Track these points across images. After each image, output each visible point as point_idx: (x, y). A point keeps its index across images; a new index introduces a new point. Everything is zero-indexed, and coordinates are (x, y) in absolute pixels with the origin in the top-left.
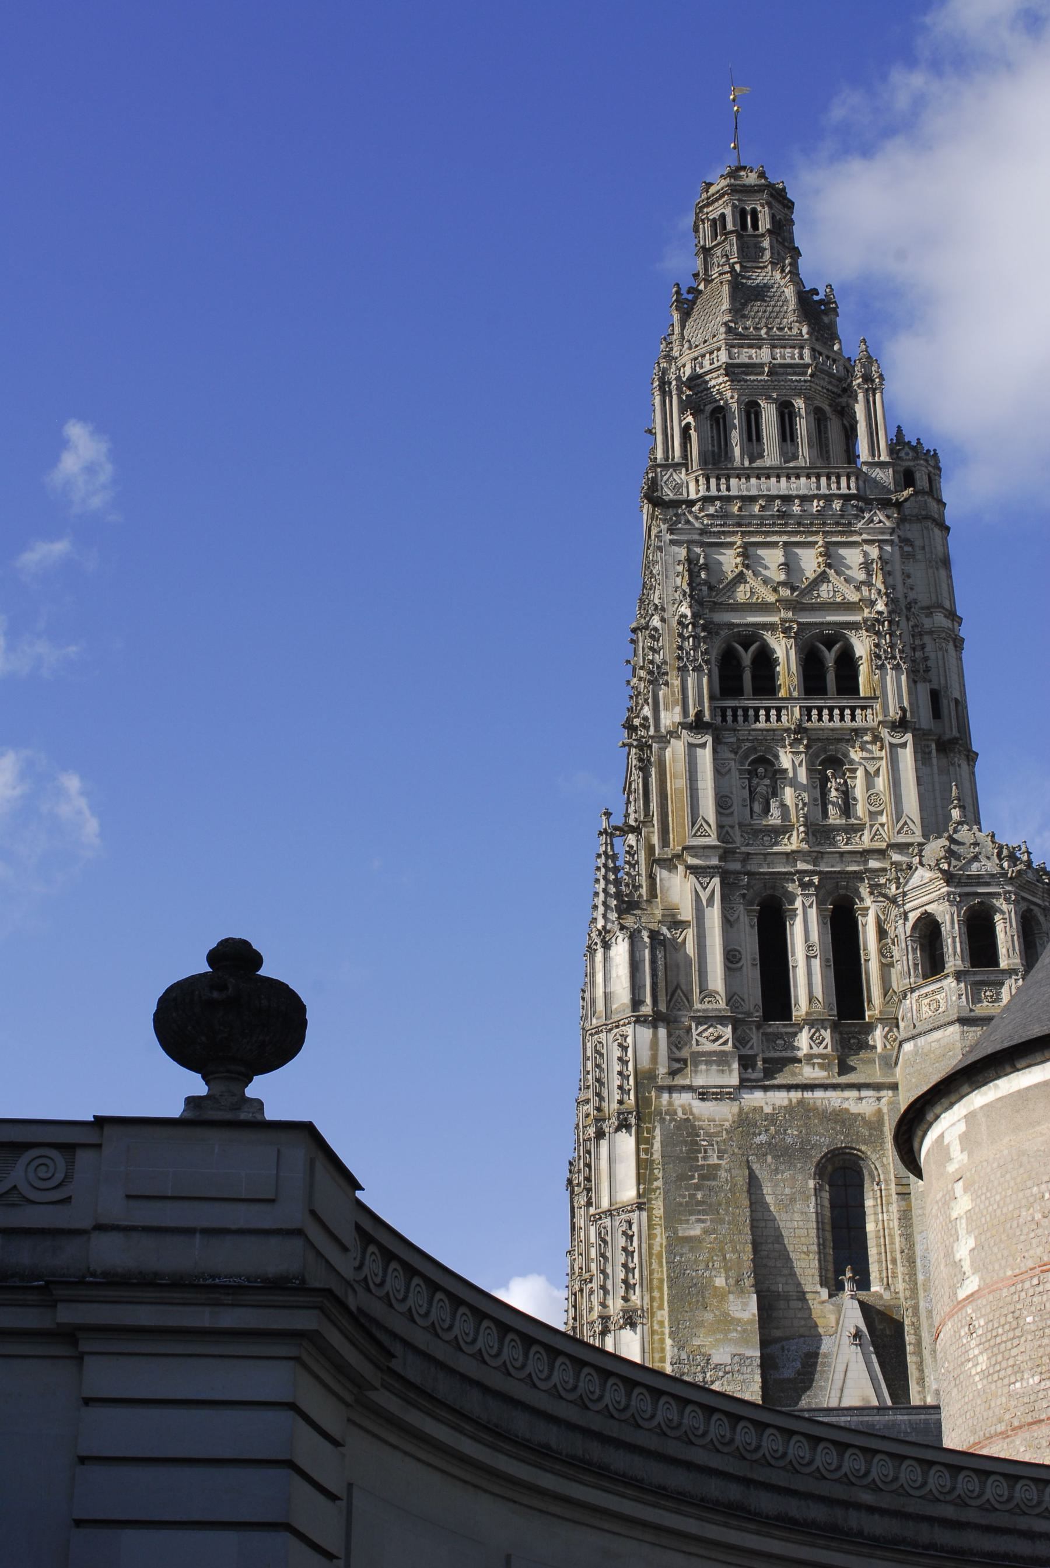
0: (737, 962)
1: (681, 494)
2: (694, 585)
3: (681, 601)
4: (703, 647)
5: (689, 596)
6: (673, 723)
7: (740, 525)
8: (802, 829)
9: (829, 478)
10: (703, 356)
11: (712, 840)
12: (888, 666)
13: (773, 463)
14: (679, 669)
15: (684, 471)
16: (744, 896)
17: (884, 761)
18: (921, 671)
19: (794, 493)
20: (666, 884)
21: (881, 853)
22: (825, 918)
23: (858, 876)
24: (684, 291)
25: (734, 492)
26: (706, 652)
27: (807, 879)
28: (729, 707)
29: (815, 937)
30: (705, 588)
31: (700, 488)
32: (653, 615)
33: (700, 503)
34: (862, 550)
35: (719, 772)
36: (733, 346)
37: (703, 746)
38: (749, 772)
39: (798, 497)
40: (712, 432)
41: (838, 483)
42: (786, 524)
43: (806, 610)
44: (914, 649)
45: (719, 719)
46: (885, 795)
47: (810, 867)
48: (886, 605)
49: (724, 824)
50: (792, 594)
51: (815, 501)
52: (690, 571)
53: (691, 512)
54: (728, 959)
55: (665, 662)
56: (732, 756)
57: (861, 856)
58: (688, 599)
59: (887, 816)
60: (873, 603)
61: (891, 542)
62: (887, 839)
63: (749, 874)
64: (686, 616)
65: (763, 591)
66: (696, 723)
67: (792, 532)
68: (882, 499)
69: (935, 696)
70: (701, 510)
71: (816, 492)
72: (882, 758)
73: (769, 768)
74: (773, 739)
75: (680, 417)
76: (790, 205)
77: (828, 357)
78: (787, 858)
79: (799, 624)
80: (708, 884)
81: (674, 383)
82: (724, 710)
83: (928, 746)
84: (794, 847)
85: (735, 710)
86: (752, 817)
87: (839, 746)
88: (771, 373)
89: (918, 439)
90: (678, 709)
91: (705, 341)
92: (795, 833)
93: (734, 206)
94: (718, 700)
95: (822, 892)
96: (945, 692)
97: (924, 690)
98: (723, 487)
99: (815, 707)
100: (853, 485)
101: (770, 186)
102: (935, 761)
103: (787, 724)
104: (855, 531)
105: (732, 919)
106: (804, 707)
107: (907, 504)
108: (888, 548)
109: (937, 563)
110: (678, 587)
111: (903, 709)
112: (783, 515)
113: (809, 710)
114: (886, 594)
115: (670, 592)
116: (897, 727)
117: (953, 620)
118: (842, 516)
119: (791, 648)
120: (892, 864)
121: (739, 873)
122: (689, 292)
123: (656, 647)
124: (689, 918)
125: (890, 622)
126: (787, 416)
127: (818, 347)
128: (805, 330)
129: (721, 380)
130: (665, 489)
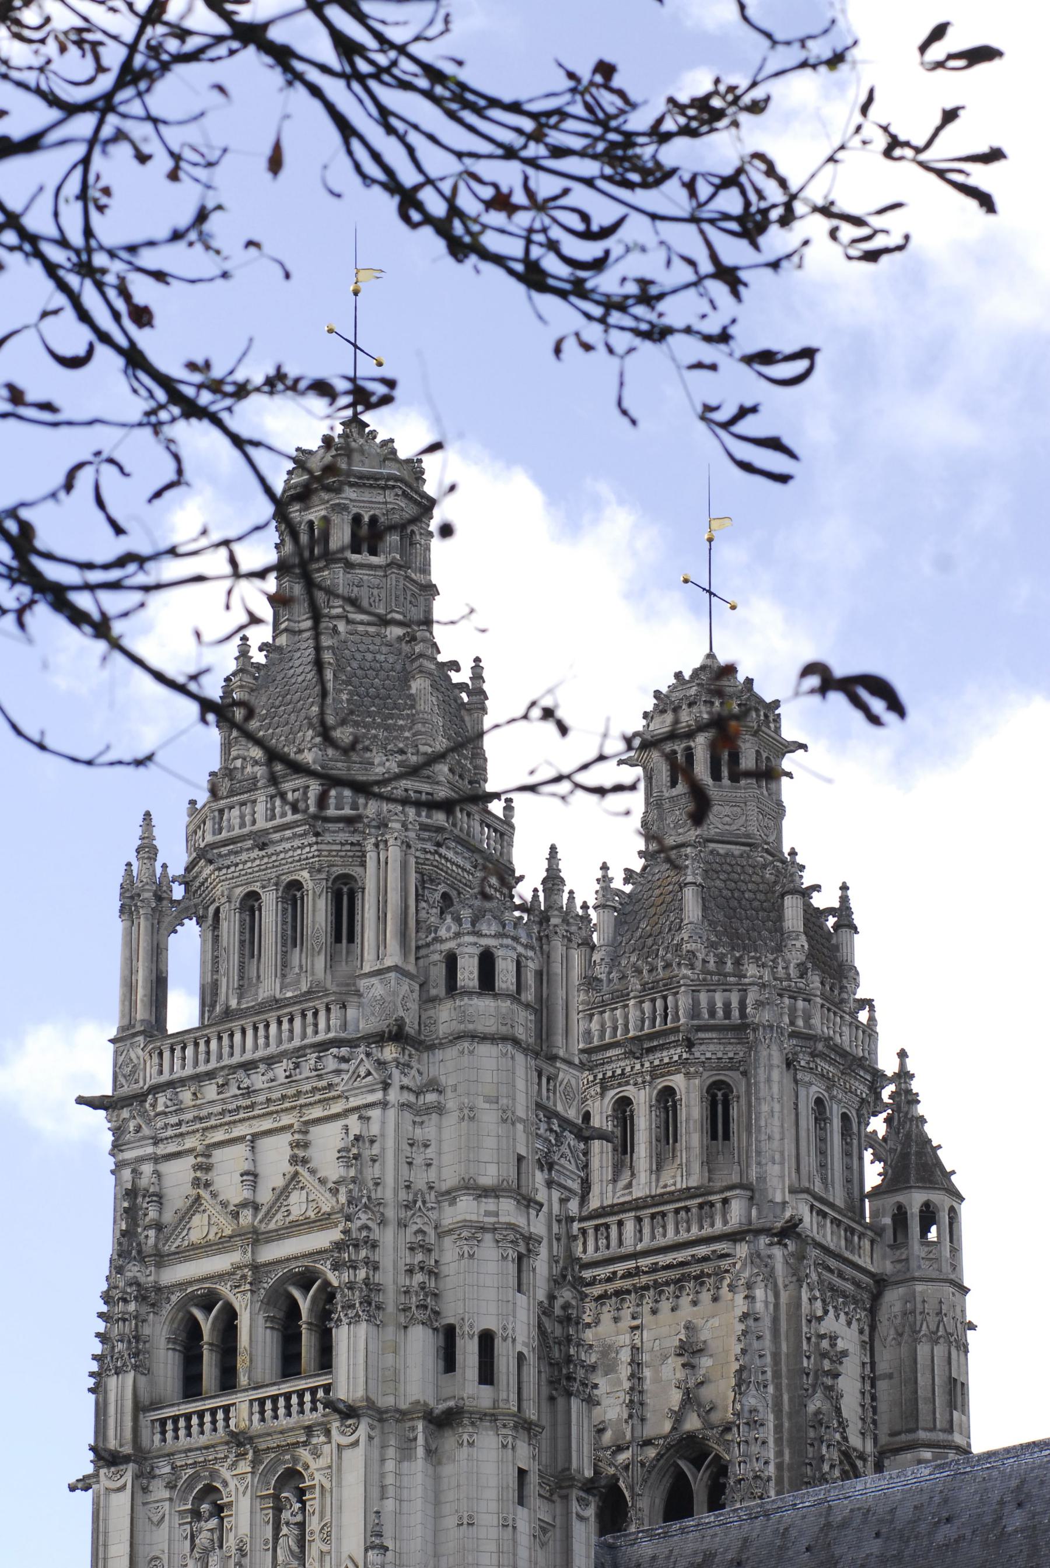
42: (252, 1106)
43: (273, 1241)
56: (166, 1494)
67: (264, 1115)
74: (216, 1458)
83: (413, 1429)
96: (461, 1327)
104: (339, 1097)
112: (249, 1092)
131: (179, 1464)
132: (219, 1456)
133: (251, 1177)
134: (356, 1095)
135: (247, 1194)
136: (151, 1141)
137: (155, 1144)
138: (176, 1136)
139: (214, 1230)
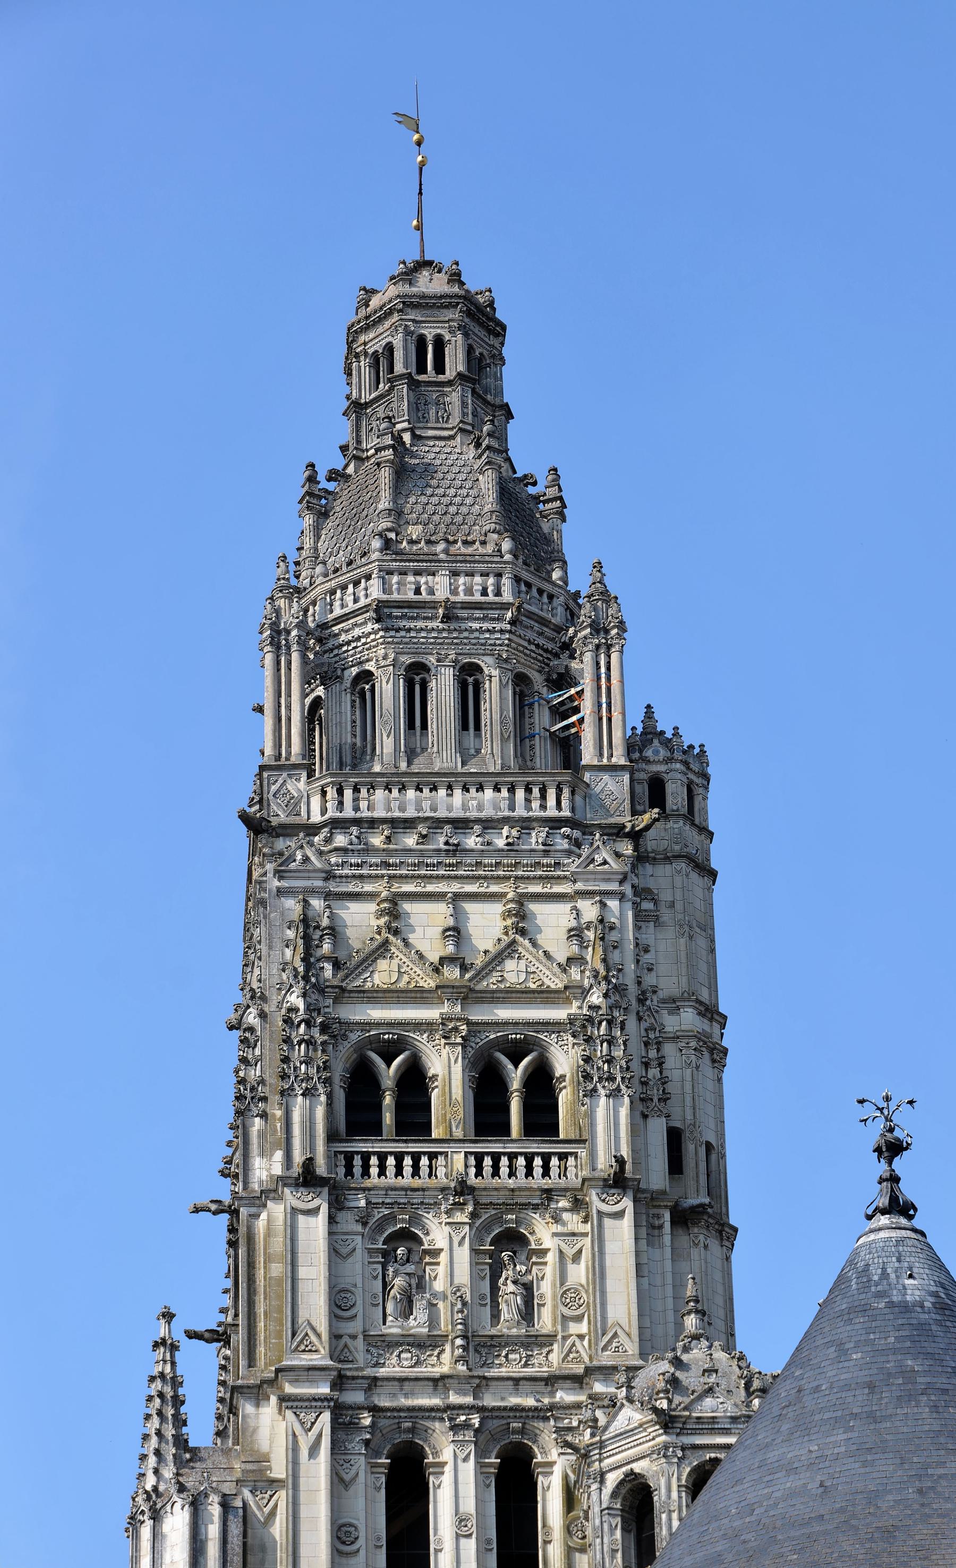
0: (352, 1543)
1: (298, 814)
2: (312, 960)
3: (291, 986)
4: (320, 1058)
5: (303, 978)
6: (271, 1176)
7: (387, 865)
8: (459, 1342)
9: (528, 790)
10: (344, 587)
11: (320, 1358)
12: (602, 1092)
13: (445, 765)
14: (282, 1093)
15: (304, 775)
16: (367, 1443)
17: (589, 1239)
18: (656, 1099)
19: (473, 814)
20: (252, 1422)
21: (578, 1381)
22: (487, 1478)
23: (540, 1414)
24: (321, 477)
25: (380, 813)
26: (326, 1067)
27: (463, 1418)
28: (357, 1153)
29: (469, 1505)
30: (328, 967)
31: (329, 805)
32: (248, 1007)
33: (326, 830)
34: (575, 908)
35: (336, 1253)
36: (390, 573)
37: (314, 1212)
38: (385, 1254)
39: (478, 821)
40: (353, 713)
41: (543, 797)
43: (483, 1002)
44: (646, 1065)
45: (342, 1171)
46: (587, 1292)
47: (468, 1400)
48: (606, 996)
49: (341, 1332)
50: (462, 976)
51: (506, 828)
52: (307, 938)
53: (311, 844)
54: (339, 1538)
55: (262, 1082)
56: (359, 1228)
57: (546, 1385)
58: (302, 983)
59: (589, 1323)
60: (585, 992)
61: (622, 897)
62: (587, 1359)
63: (375, 1410)
64: (296, 1010)
65: (419, 972)
66: (305, 1178)
67: (468, 877)
68: (610, 826)
69: (675, 1138)
70: (328, 840)
71: (507, 813)
72: (586, 1235)
73: (414, 1247)
75: (303, 690)
76: (498, 330)
77: (540, 592)
78: (436, 1386)
79: (469, 1023)
80: (313, 1424)
81: (294, 633)
82: (349, 1157)
83: (658, 1217)
84: (445, 1369)
85: (366, 1157)
86: (384, 1323)
87: (522, 1215)
88: (447, 618)
89: (676, 728)
90: (279, 1155)
91: (350, 563)
92: (448, 1347)
93: (408, 332)
94: (341, 1141)
95: (482, 1438)
97: (657, 1129)
98: (363, 805)
99: (488, 1154)
100: (565, 803)
101: (468, 298)
102: (667, 1239)
103: (445, 1180)
104: (565, 877)
105: (347, 1478)
106: (471, 1153)
107: (651, 833)
108: (613, 904)
109: (691, 927)
110: (286, 964)
111: (620, 1161)
112: (455, 850)
113: (479, 1158)
114: (606, 978)
115: (275, 971)
116: (611, 1187)
117: (711, 1020)
118: (546, 853)
119: (456, 1061)
120: (590, 1397)
121: (361, 1408)
122: (329, 479)
123: (250, 1056)
124: (283, 1476)
125: (610, 1023)
126: (471, 688)
127: (525, 575)
128: (506, 545)
129: (369, 627)
130: (274, 807)
131: (374, 1201)
132: (426, 1201)
133: (456, 933)
134: (587, 880)
135: (450, 949)
136: (324, 875)
137: (326, 879)
138: (354, 876)
139: (406, 978)
